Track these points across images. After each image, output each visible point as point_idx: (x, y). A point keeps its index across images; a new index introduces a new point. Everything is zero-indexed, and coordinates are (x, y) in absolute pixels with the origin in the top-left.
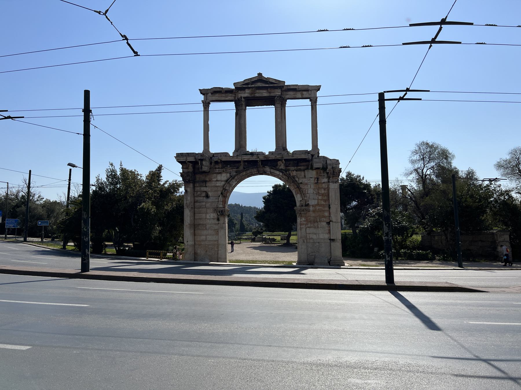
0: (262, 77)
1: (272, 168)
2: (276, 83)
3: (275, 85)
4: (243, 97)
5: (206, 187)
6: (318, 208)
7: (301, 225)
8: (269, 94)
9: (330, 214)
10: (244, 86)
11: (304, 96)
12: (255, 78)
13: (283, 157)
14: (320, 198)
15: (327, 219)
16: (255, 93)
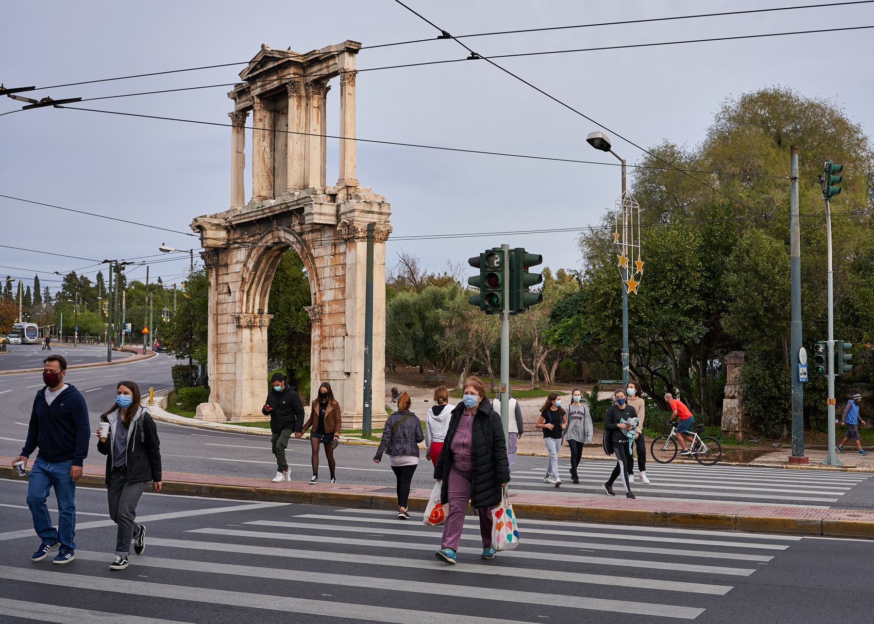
0: (267, 52)
1: (285, 231)
2: (281, 57)
3: (280, 62)
4: (256, 96)
5: (227, 274)
6: (335, 307)
7: (314, 345)
8: (279, 81)
9: (345, 320)
10: (250, 76)
11: (332, 70)
12: (259, 56)
13: (288, 207)
14: (337, 285)
15: (343, 331)
16: (266, 85)
